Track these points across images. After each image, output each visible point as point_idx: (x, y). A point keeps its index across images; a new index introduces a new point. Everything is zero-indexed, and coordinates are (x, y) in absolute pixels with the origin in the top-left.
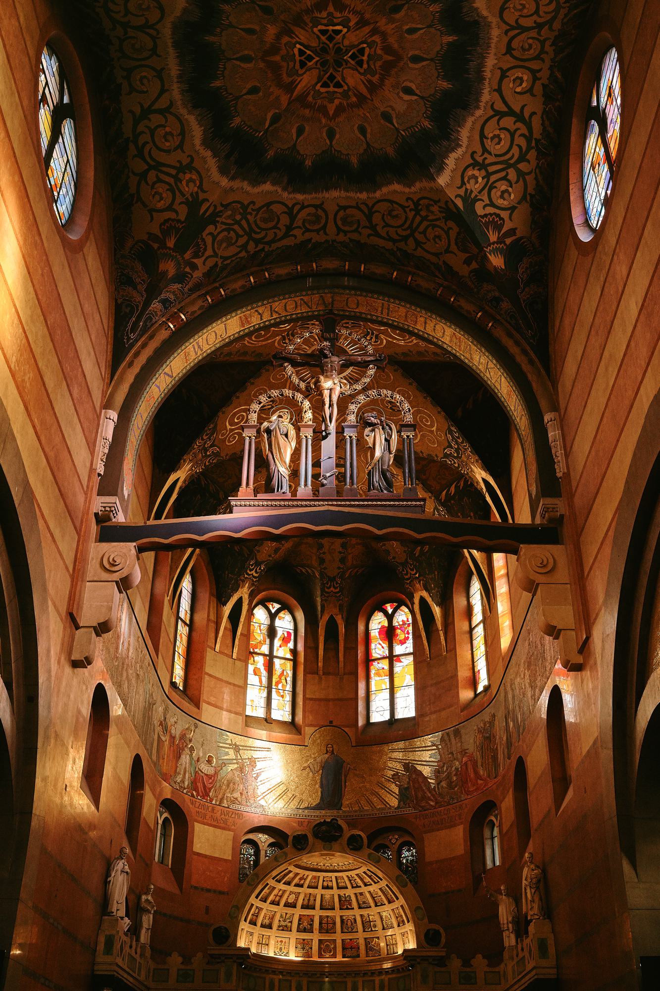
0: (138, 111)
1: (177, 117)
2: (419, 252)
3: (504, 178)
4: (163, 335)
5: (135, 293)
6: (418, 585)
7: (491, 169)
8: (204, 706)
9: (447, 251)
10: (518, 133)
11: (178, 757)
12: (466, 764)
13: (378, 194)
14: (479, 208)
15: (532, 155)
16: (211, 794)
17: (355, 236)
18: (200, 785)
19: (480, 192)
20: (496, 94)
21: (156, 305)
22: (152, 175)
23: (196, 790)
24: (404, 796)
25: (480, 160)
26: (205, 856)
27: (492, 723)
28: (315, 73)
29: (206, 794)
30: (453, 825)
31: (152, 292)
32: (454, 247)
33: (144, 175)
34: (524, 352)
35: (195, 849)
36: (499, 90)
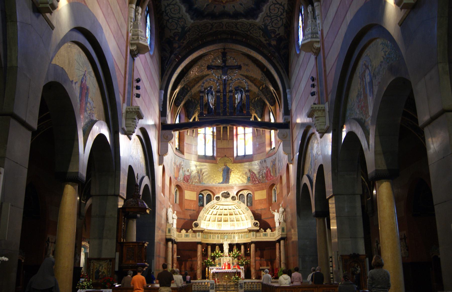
0: (166, 5)
1: (178, 5)
2: (251, 35)
3: (276, 20)
4: (175, 63)
6: (253, 112)
8: (185, 154)
11: (179, 171)
12: (267, 171)
13: (238, 21)
14: (269, 28)
15: (285, 14)
16: (189, 181)
18: (186, 179)
19: (269, 23)
21: (173, 56)
22: (170, 21)
23: (184, 180)
26: (189, 200)
27: (275, 160)
29: (187, 181)
31: (171, 52)
32: (261, 36)
33: (168, 20)
34: (282, 68)
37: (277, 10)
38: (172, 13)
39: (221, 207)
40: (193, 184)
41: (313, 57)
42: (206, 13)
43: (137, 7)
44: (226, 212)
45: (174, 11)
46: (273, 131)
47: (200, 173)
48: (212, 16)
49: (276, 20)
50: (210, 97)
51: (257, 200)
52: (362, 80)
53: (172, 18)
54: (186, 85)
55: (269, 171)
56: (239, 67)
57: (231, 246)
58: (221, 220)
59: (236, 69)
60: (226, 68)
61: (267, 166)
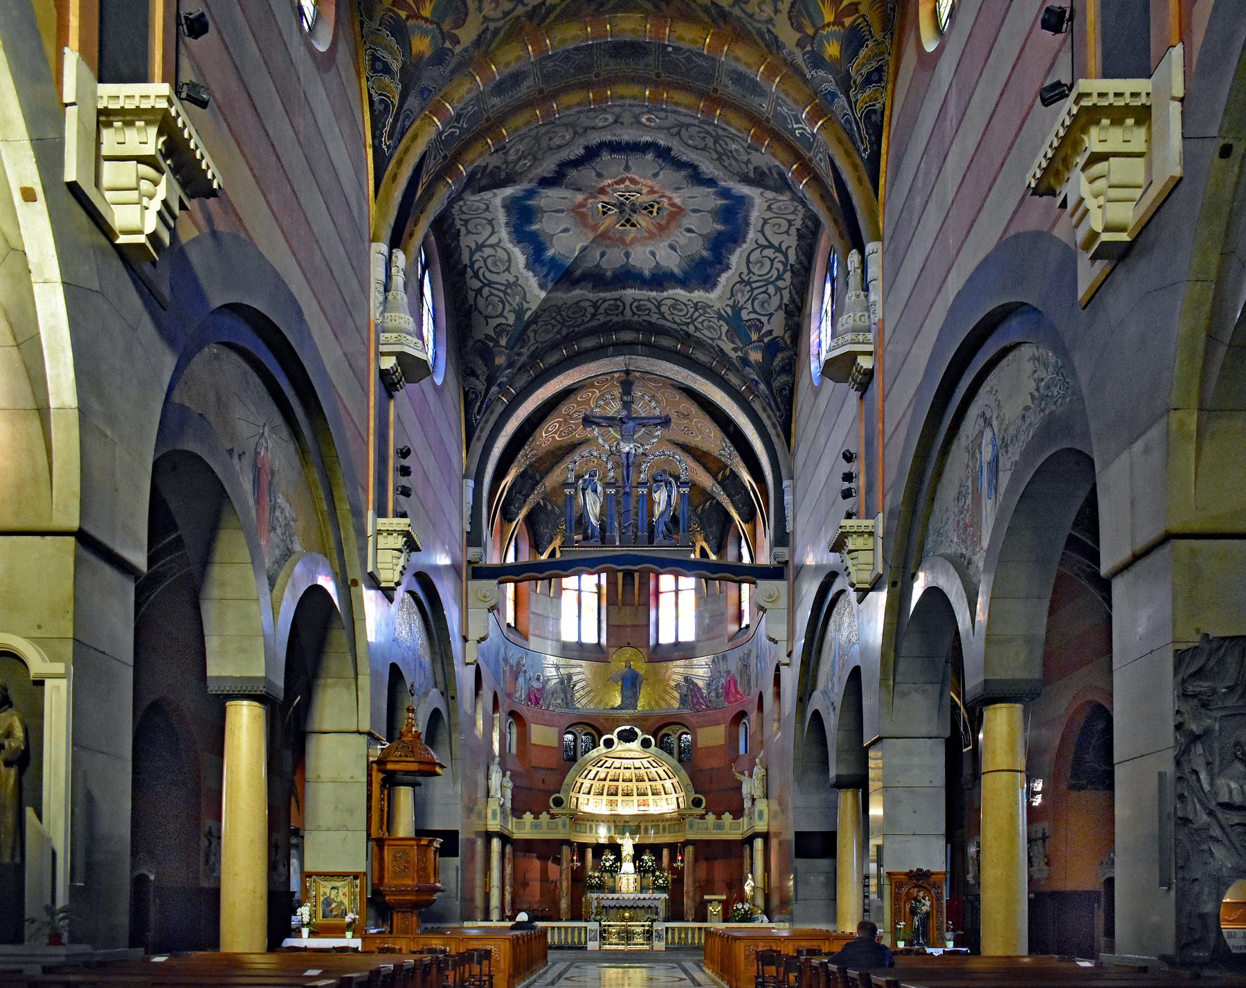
0: (473, 246)
1: (505, 249)
2: (698, 334)
3: (765, 292)
5: (477, 382)
6: (699, 537)
7: (754, 285)
8: (531, 638)
9: (720, 338)
10: (776, 260)
13: (665, 294)
15: (788, 276)
17: (648, 318)
18: (533, 697)
20: (760, 234)
22: (486, 291)
23: (530, 700)
24: (683, 700)
25: (746, 278)
27: (749, 655)
28: (614, 218)
29: (537, 703)
30: (718, 724)
32: (724, 337)
33: (479, 291)
35: (533, 742)
36: (762, 232)
37: (768, 263)
38: (491, 271)
39: (617, 763)
40: (551, 709)
41: (854, 395)
42: (578, 272)
43: (394, 251)
44: (627, 774)
46: (745, 587)
47: (566, 684)
48: (597, 279)
49: (765, 292)
50: (590, 497)
51: (701, 749)
52: (973, 455)
53: (490, 284)
54: (530, 466)
55: (732, 682)
56: (665, 422)
57: (639, 849)
58: (617, 791)
59: (657, 425)
60: (631, 424)
61: (729, 668)
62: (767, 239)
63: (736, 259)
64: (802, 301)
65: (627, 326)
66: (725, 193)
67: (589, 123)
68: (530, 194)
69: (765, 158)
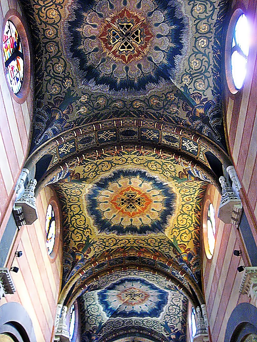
2: (155, 330)
9: (162, 331)
13: (144, 318)
14: (169, 324)
15: (181, 313)
19: (169, 320)
22: (91, 317)
33: (89, 317)
45: (94, 310)
48: (124, 314)
62: (174, 303)
63: (165, 308)
64: (186, 320)
65: (133, 327)
66: (160, 291)
67: (122, 275)
68: (105, 291)
69: (170, 283)
